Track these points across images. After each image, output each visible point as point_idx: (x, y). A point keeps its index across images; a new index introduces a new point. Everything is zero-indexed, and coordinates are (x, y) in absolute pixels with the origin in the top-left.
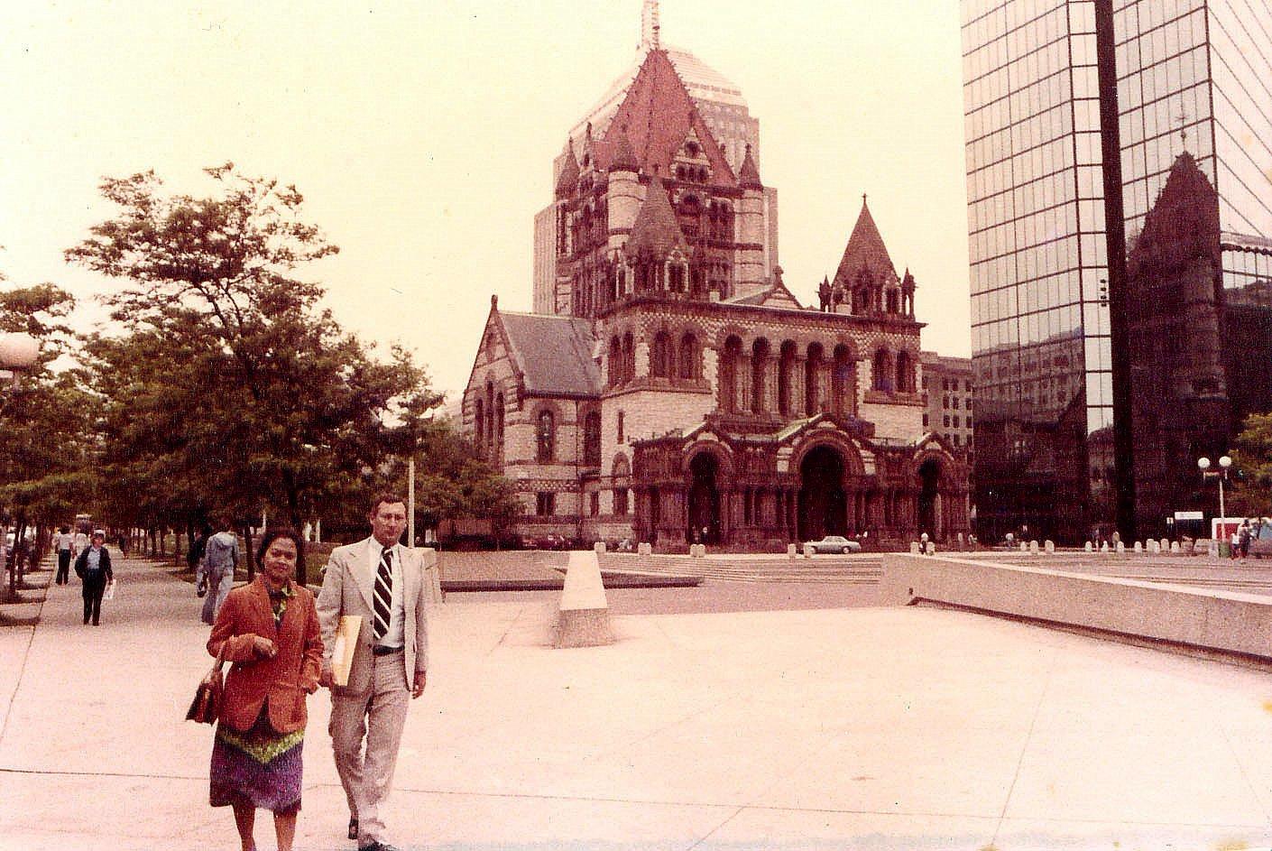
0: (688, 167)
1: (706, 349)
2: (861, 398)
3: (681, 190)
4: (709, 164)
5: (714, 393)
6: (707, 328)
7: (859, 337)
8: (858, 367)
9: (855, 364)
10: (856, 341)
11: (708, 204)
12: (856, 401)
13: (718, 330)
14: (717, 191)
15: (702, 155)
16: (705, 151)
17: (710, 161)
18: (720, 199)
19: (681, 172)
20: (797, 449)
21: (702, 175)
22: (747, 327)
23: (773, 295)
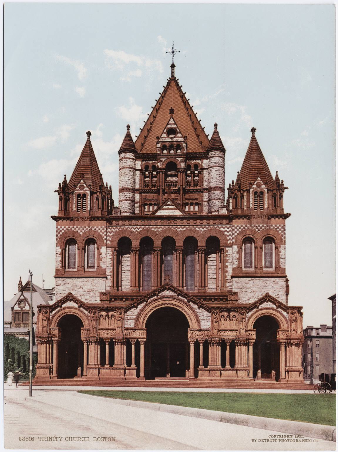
0: (168, 144)
1: (103, 247)
2: (229, 275)
3: (163, 160)
4: (183, 140)
5: (109, 277)
6: (103, 233)
7: (228, 230)
8: (227, 251)
9: (223, 249)
10: (226, 233)
11: (183, 165)
12: (225, 277)
13: (112, 234)
14: (188, 156)
15: (179, 135)
16: (180, 132)
17: (185, 138)
18: (193, 162)
19: (164, 147)
20: (141, 311)
21: (179, 147)
22: (134, 231)
23: (164, 207)
